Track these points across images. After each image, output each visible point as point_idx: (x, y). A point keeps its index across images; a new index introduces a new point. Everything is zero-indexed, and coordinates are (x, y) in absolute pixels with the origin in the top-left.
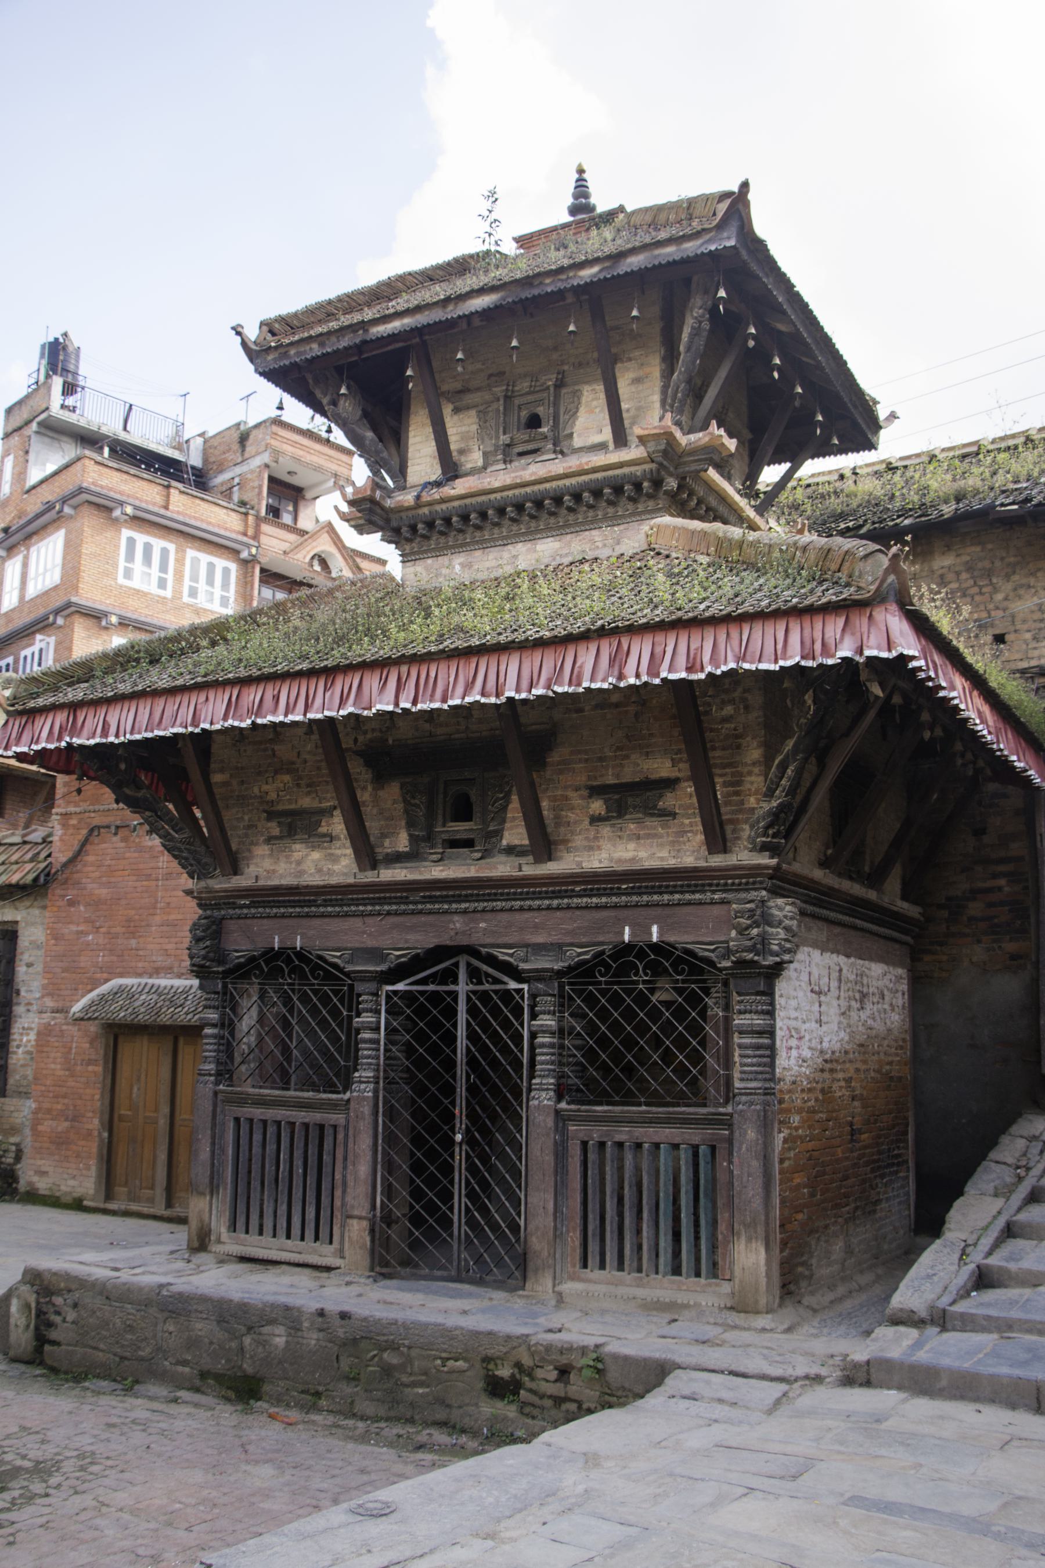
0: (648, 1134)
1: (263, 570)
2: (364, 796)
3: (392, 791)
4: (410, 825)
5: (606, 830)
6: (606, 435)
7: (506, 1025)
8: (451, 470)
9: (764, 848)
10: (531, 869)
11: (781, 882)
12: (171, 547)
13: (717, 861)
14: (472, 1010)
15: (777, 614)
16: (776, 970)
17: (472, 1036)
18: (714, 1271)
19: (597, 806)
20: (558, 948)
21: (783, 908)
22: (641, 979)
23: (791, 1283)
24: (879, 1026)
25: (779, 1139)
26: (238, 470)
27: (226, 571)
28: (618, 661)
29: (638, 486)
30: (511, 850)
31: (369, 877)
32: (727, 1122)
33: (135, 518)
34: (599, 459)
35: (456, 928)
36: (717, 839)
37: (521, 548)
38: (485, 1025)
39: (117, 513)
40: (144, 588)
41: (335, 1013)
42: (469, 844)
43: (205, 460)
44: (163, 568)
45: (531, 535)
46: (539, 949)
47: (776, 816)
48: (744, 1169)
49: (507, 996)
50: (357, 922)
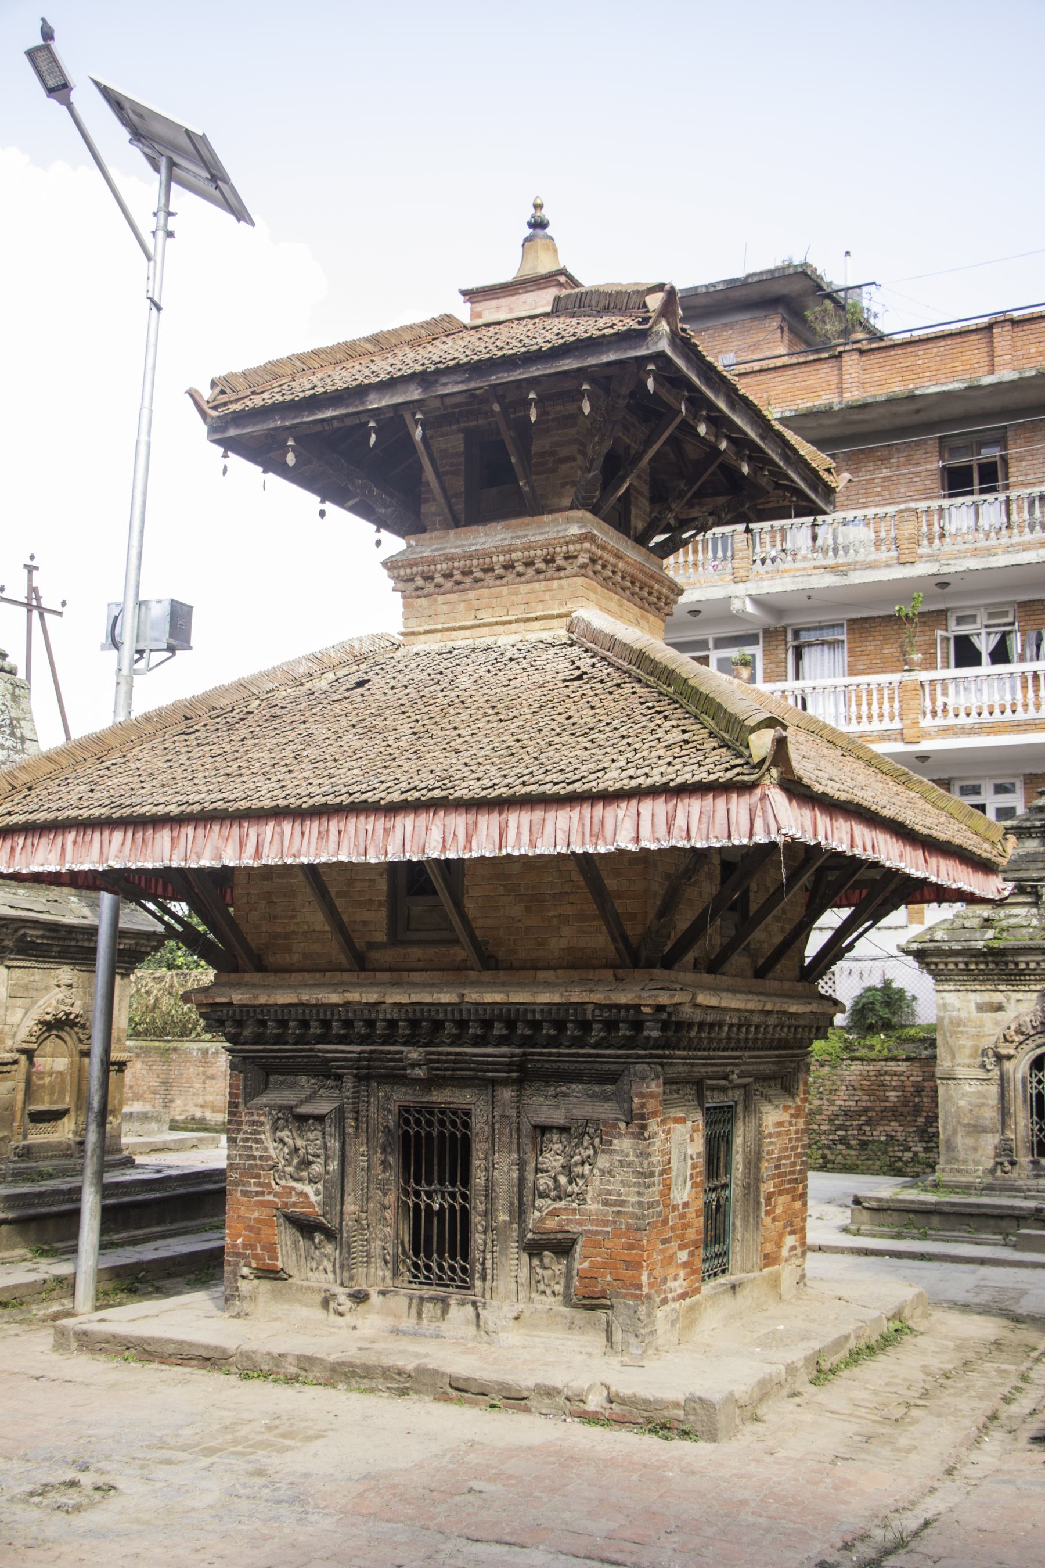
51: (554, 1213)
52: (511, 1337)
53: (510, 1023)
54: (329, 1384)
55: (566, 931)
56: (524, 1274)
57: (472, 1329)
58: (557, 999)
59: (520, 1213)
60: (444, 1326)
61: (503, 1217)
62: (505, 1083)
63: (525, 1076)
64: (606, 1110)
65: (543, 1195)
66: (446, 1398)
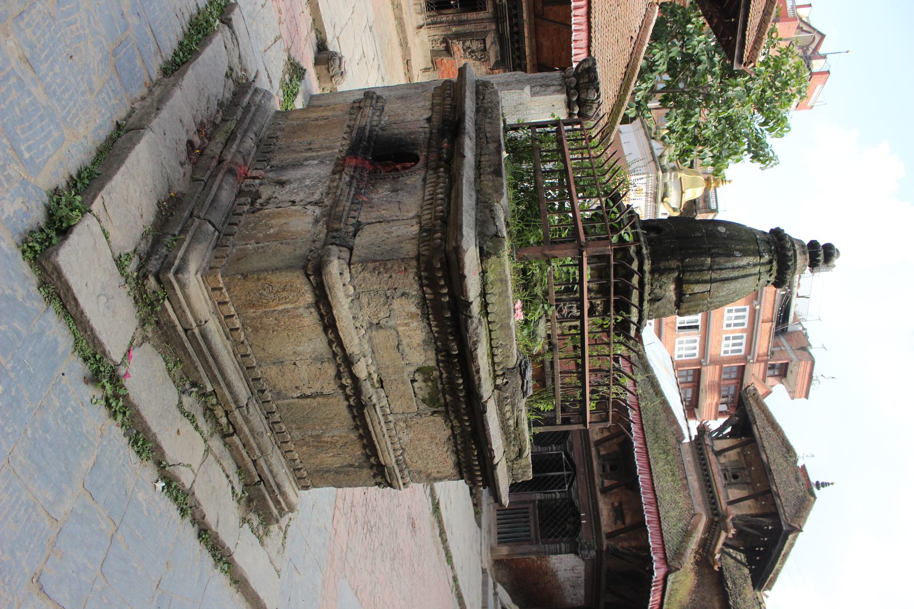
0: (532, 523)
1: (744, 367)
2: (615, 441)
3: (616, 448)
4: (608, 454)
5: (610, 507)
6: (731, 499)
7: (556, 485)
8: (718, 454)
9: (608, 547)
10: (598, 488)
11: (599, 552)
12: (746, 327)
13: (604, 536)
14: (559, 476)
15: (663, 541)
16: (577, 554)
17: (553, 476)
18: (499, 543)
19: (616, 504)
20: (578, 497)
21: (593, 553)
22: (572, 519)
23: (498, 563)
24: (566, 593)
25: (534, 557)
26: (788, 348)
27: (740, 351)
28: (649, 504)
29: (715, 509)
30: (603, 482)
31: (592, 445)
32: (537, 543)
33: (755, 310)
34: (722, 498)
35: (581, 470)
36: (609, 536)
37: (695, 477)
38: (555, 480)
39: (755, 302)
40: (725, 318)
41: (555, 439)
42: (604, 471)
43: (792, 333)
44: (735, 325)
45: (699, 480)
46: (577, 492)
47: (616, 549)
48: (526, 548)
49: (564, 485)
50: (580, 442)
51: (459, 50)
52: (417, 41)
53: (517, 35)
54: (396, 18)
55: (548, 43)
56: (436, 37)
57: (415, 25)
58: (527, 53)
59: (458, 36)
60: (414, 15)
61: (454, 29)
62: (497, 26)
63: (501, 38)
64: (493, 60)
65: (464, 43)
66: (404, 59)
